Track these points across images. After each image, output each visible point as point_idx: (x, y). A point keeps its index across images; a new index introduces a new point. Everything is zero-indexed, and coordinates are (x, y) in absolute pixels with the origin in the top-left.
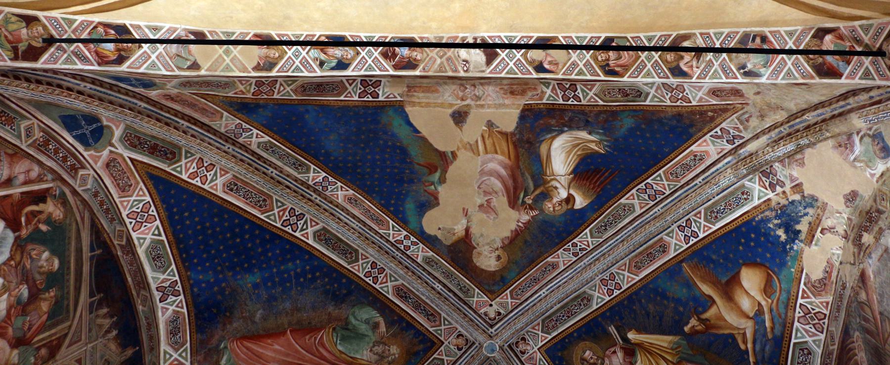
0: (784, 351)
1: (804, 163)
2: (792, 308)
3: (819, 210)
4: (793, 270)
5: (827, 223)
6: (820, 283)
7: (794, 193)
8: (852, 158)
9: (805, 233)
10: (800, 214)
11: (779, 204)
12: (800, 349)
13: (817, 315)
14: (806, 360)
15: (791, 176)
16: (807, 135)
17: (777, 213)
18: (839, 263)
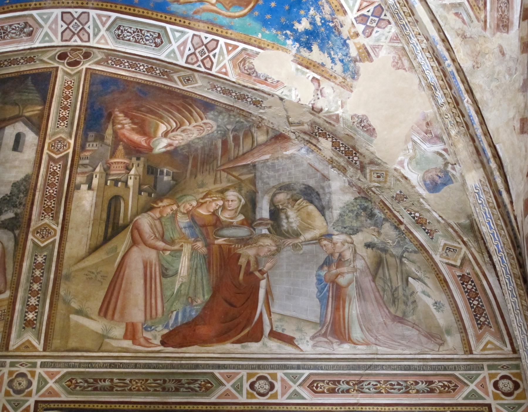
0: (152, 14)
1: (399, 69)
2: (210, 30)
3: (340, 79)
4: (260, 36)
5: (327, 87)
6: (251, 69)
7: (358, 49)
8: (415, 139)
9: (310, 57)
10: (332, 53)
11: (342, 26)
12: (159, 34)
13: (208, 59)
14: (148, 40)
15: (379, 47)
16: (449, 103)
17: (329, 22)
18: (281, 96)
